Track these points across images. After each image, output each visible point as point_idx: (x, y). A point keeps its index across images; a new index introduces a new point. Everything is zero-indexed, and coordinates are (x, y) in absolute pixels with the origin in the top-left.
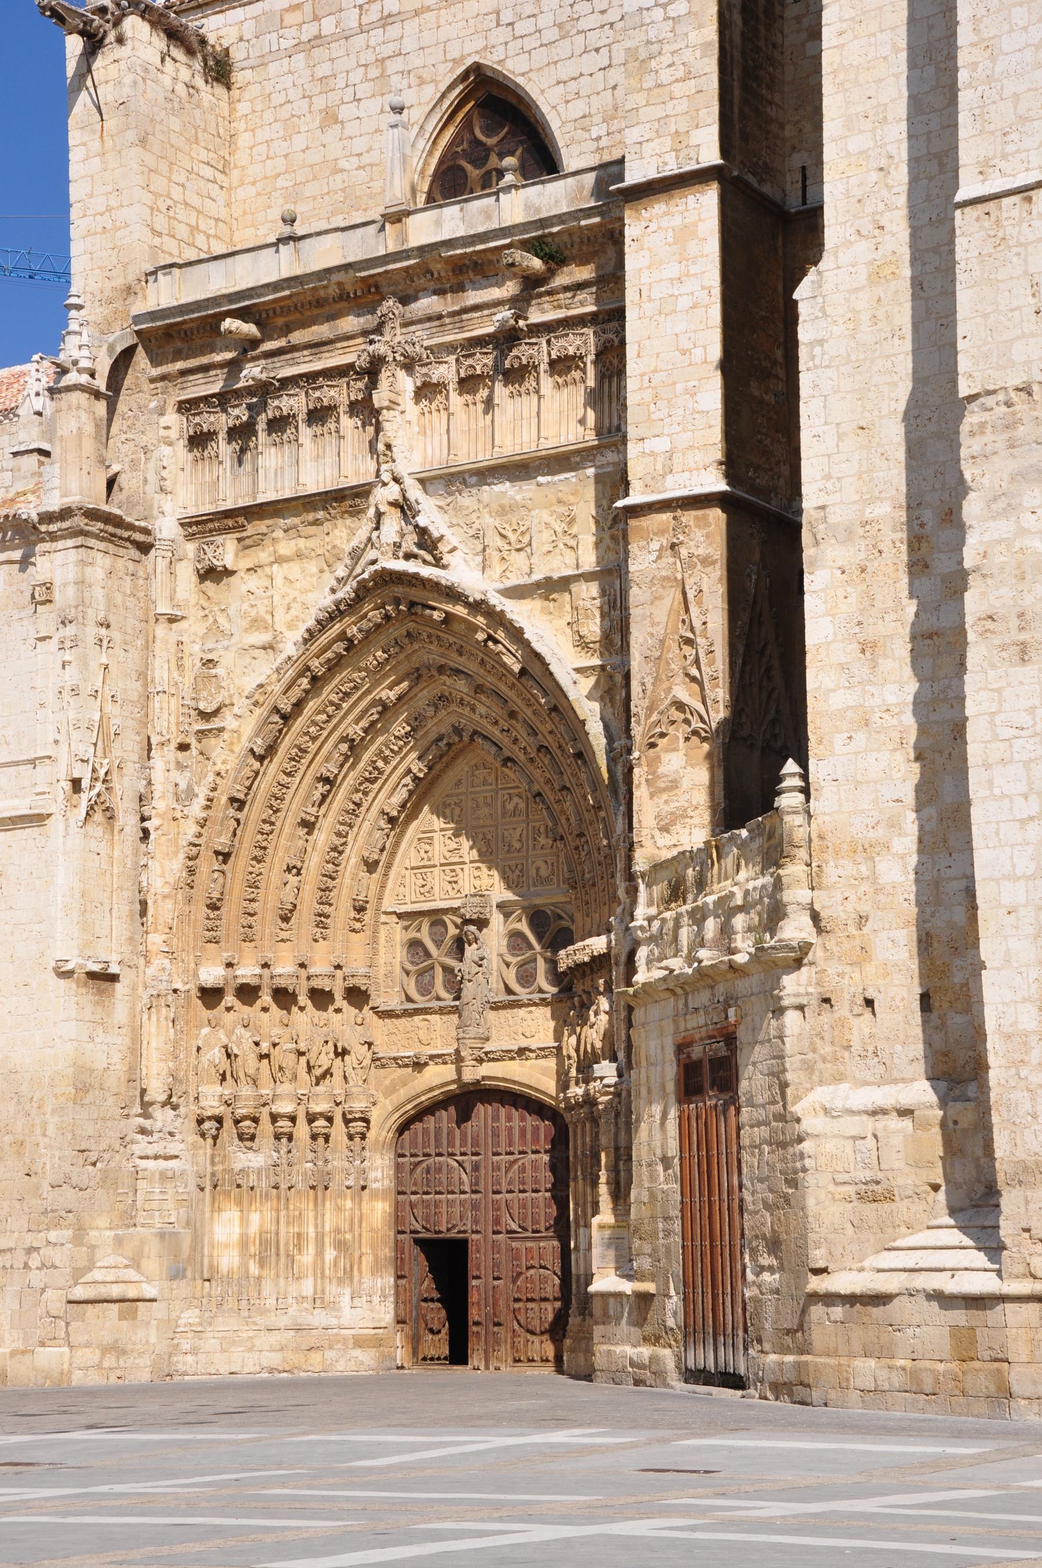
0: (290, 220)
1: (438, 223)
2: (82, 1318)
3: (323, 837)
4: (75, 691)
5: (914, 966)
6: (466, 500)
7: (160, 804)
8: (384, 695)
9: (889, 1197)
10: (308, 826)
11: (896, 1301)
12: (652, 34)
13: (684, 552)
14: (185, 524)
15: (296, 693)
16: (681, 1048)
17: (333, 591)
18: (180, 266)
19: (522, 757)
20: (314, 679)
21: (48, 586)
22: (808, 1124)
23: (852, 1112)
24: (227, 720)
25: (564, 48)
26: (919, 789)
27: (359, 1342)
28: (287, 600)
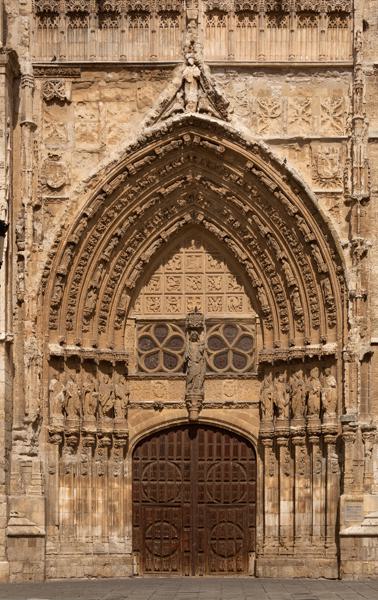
2: (13, 545)
8: (162, 191)
15: (116, 182)
17: (148, 124)
20: (129, 175)
24: (67, 193)
27: (126, 561)
28: (108, 126)
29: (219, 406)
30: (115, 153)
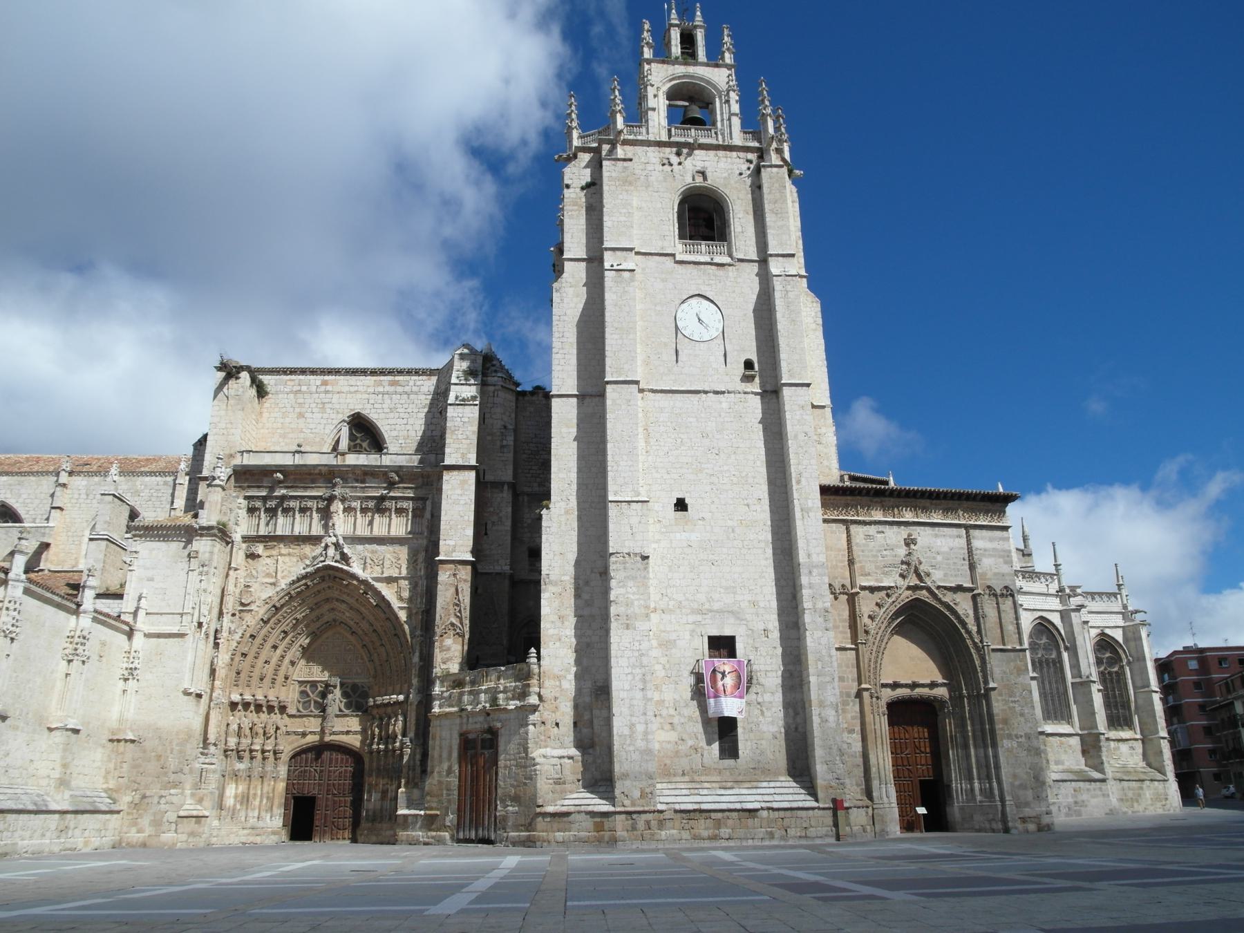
0: (299, 446)
1: (358, 458)
3: (279, 652)
4: (205, 591)
5: (572, 713)
6: (360, 547)
7: (225, 634)
9: (564, 783)
10: (275, 647)
11: (573, 815)
12: (456, 424)
13: (458, 577)
14: (243, 537)
15: (283, 601)
16: (461, 735)
17: (304, 569)
18: (253, 452)
19: (361, 632)
20: (291, 597)
21: (197, 552)
22: (538, 760)
23: (553, 757)
24: (253, 607)
25: (392, 415)
26: (575, 661)
27: (274, 833)
29: (342, 733)
30: (283, 584)
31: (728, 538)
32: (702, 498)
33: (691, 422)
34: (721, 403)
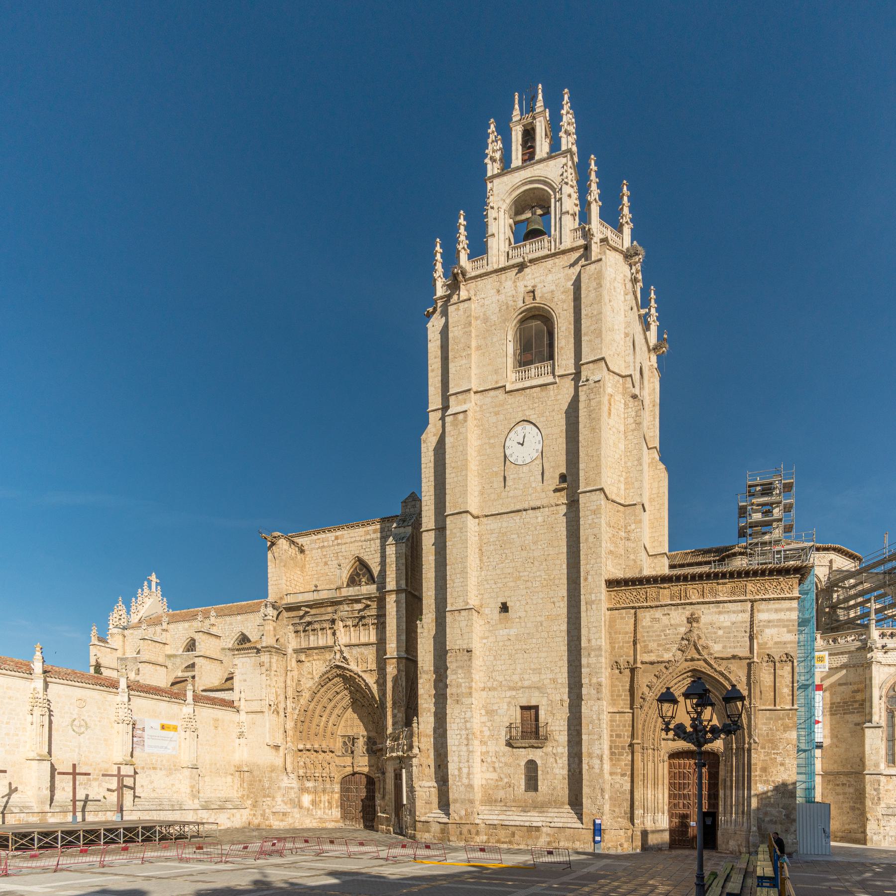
31: (537, 631)
32: (519, 601)
33: (513, 539)
34: (537, 518)
